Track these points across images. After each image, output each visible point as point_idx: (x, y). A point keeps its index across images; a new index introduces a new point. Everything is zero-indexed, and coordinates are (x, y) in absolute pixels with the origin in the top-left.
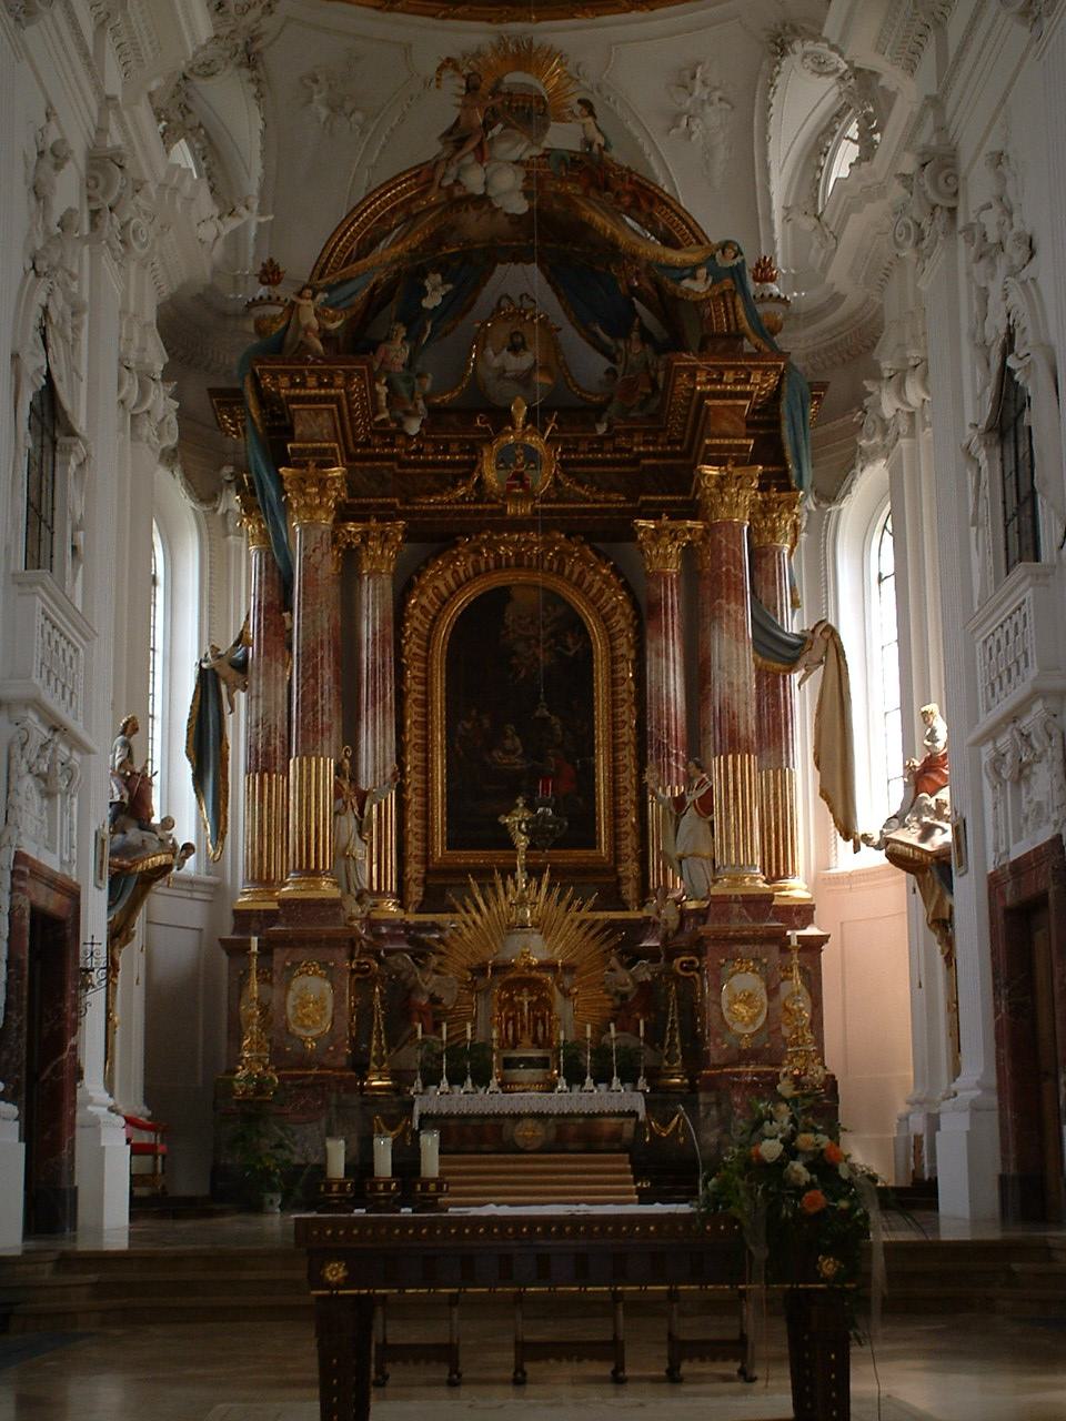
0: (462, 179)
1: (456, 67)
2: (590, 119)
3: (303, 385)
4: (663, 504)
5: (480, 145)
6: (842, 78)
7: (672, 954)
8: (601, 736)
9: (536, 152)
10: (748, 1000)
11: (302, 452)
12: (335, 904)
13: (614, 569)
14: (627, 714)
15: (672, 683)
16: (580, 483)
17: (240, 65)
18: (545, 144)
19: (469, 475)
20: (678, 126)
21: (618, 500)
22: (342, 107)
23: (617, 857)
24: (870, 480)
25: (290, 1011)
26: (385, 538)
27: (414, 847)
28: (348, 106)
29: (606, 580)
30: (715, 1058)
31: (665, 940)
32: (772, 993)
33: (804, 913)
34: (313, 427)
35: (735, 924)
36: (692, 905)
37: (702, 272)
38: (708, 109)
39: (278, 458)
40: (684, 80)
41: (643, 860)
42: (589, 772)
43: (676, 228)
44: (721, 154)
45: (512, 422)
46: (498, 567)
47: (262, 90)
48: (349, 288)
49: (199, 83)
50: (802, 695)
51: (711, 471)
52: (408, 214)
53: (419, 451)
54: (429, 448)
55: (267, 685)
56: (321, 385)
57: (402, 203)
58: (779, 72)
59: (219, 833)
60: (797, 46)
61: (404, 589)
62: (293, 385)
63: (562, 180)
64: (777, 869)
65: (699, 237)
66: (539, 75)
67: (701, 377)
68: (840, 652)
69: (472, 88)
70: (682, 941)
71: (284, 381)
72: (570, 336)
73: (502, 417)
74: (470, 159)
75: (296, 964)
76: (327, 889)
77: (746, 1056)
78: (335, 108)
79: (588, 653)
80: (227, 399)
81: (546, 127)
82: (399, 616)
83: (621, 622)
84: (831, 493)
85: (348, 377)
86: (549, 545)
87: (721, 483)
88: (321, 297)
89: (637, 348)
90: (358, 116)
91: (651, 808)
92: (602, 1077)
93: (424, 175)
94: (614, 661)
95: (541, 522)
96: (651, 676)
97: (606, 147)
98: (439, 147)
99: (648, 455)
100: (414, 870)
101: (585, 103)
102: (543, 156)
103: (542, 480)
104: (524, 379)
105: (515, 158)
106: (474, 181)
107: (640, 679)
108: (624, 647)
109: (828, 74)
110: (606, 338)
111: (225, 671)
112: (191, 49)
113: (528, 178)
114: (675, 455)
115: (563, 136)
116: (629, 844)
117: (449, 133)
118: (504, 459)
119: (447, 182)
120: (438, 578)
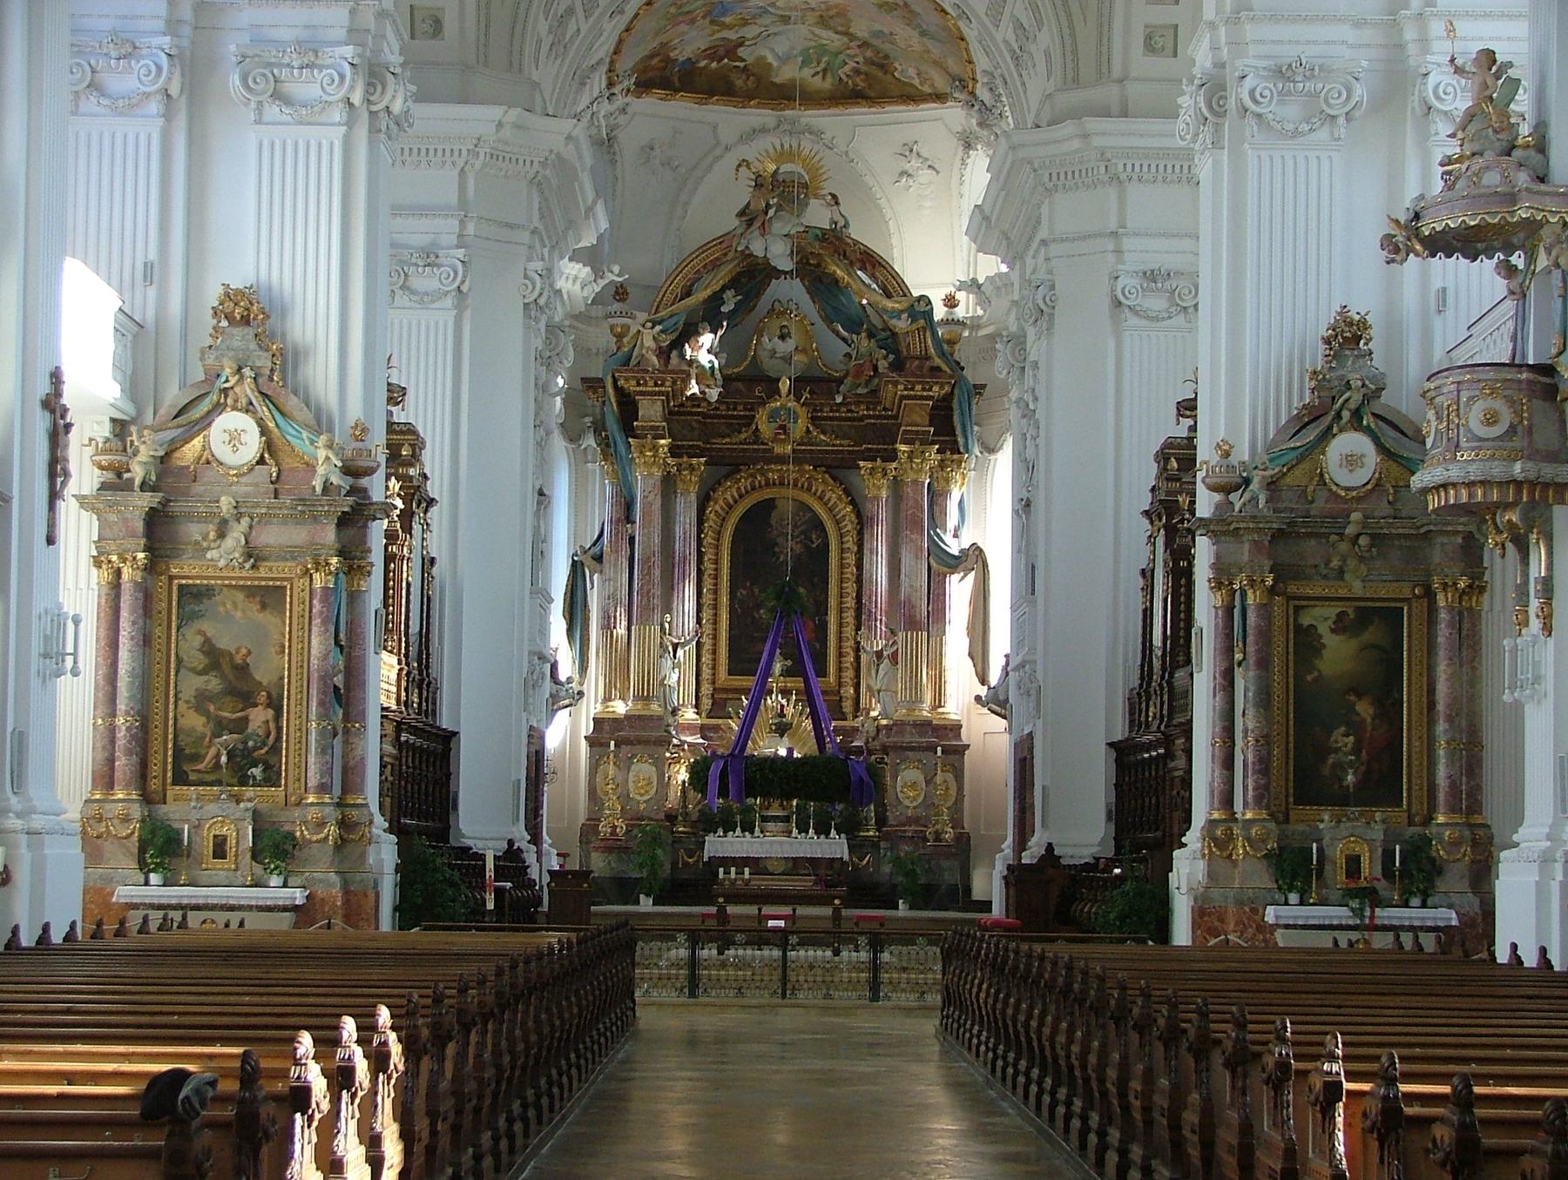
1: (748, 166)
3: (646, 384)
4: (878, 451)
7: (870, 753)
8: (832, 602)
10: (914, 785)
11: (643, 428)
12: (660, 718)
13: (847, 492)
14: (850, 588)
15: (880, 572)
16: (824, 433)
19: (749, 425)
21: (844, 445)
23: (840, 685)
24: (1003, 463)
25: (631, 784)
26: (692, 468)
27: (706, 673)
29: (840, 498)
30: (891, 821)
31: (867, 742)
32: (928, 782)
33: (956, 728)
34: (650, 411)
35: (908, 738)
36: (884, 722)
37: (904, 316)
39: (629, 430)
41: (857, 687)
42: (823, 628)
43: (892, 285)
45: (778, 392)
46: (767, 484)
48: (674, 319)
50: (959, 590)
51: (903, 448)
52: (715, 265)
53: (716, 409)
54: (723, 407)
55: (616, 572)
56: (656, 385)
59: (583, 668)
61: (704, 502)
62: (639, 384)
64: (938, 702)
65: (904, 291)
67: (901, 387)
68: (985, 565)
69: (758, 186)
70: (876, 745)
71: (634, 383)
72: (821, 325)
73: (774, 392)
74: (757, 233)
75: (634, 756)
76: (655, 708)
77: (910, 821)
79: (825, 548)
80: (592, 384)
82: (701, 521)
83: (849, 525)
84: (991, 450)
85: (674, 382)
86: (802, 472)
87: (911, 456)
88: (658, 328)
89: (865, 343)
91: (864, 657)
92: (823, 830)
94: (842, 551)
95: (799, 458)
96: (866, 566)
97: (846, 226)
98: (736, 222)
99: (869, 417)
100: (706, 689)
101: (834, 196)
103: (799, 427)
104: (787, 359)
106: (757, 248)
107: (859, 566)
108: (850, 542)
110: (845, 334)
111: (588, 561)
114: (888, 417)
115: (818, 216)
116: (849, 675)
118: (773, 416)
120: (727, 493)
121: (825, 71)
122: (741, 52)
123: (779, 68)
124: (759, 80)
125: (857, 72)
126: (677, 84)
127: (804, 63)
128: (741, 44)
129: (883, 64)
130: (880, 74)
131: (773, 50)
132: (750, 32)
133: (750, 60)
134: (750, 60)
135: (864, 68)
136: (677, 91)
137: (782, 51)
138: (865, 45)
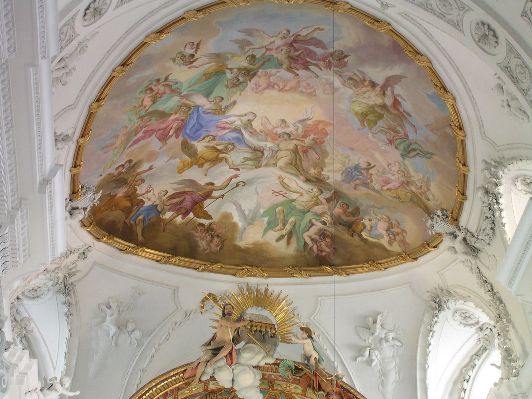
0: (216, 377)
2: (309, 341)
5: (230, 354)
6: (481, 329)
9: (271, 361)
17: (59, 291)
18: (276, 356)
20: (362, 355)
22: (126, 326)
28: (131, 326)
38: (385, 345)
40: (368, 324)
44: (393, 376)
47: (71, 312)
49: (26, 302)
57: (172, 391)
58: (436, 322)
60: (451, 304)
63: (288, 381)
66: (270, 311)
74: (223, 363)
78: (121, 326)
81: (276, 345)
90: (137, 334)
93: (187, 373)
97: (318, 361)
102: (274, 364)
105: (255, 365)
106: (224, 379)
109: (471, 325)
112: (61, 249)
113: (263, 378)
115: (289, 353)
117: (209, 344)
119: (204, 378)
121: (290, 234)
122: (209, 206)
123: (243, 231)
124: (223, 242)
125: (323, 234)
126: (140, 238)
127: (271, 226)
128: (208, 195)
129: (350, 221)
130: (346, 236)
131: (239, 207)
132: (220, 175)
133: (216, 218)
134: (216, 218)
135: (331, 229)
136: (140, 245)
137: (253, 202)
138: (336, 196)
